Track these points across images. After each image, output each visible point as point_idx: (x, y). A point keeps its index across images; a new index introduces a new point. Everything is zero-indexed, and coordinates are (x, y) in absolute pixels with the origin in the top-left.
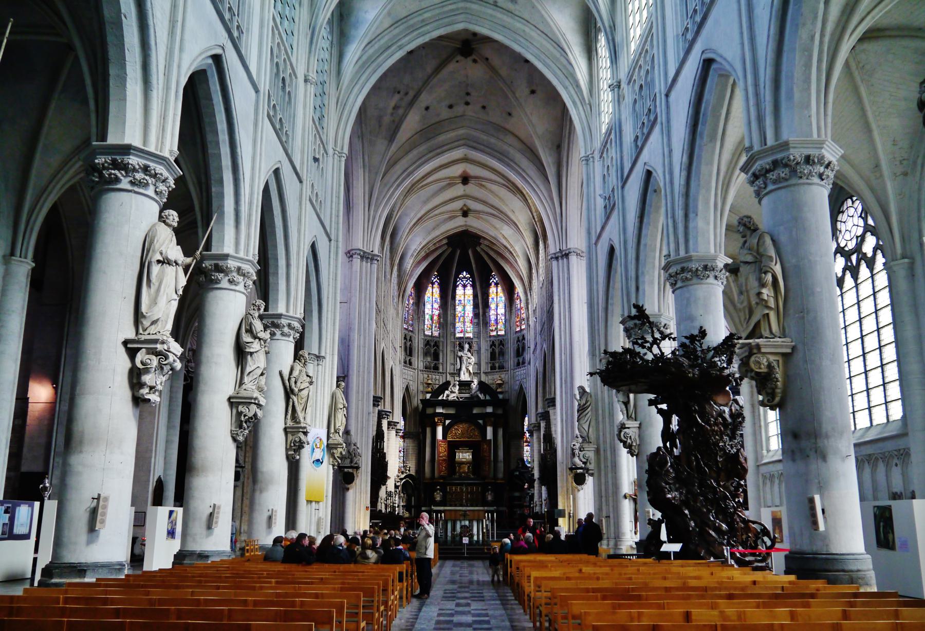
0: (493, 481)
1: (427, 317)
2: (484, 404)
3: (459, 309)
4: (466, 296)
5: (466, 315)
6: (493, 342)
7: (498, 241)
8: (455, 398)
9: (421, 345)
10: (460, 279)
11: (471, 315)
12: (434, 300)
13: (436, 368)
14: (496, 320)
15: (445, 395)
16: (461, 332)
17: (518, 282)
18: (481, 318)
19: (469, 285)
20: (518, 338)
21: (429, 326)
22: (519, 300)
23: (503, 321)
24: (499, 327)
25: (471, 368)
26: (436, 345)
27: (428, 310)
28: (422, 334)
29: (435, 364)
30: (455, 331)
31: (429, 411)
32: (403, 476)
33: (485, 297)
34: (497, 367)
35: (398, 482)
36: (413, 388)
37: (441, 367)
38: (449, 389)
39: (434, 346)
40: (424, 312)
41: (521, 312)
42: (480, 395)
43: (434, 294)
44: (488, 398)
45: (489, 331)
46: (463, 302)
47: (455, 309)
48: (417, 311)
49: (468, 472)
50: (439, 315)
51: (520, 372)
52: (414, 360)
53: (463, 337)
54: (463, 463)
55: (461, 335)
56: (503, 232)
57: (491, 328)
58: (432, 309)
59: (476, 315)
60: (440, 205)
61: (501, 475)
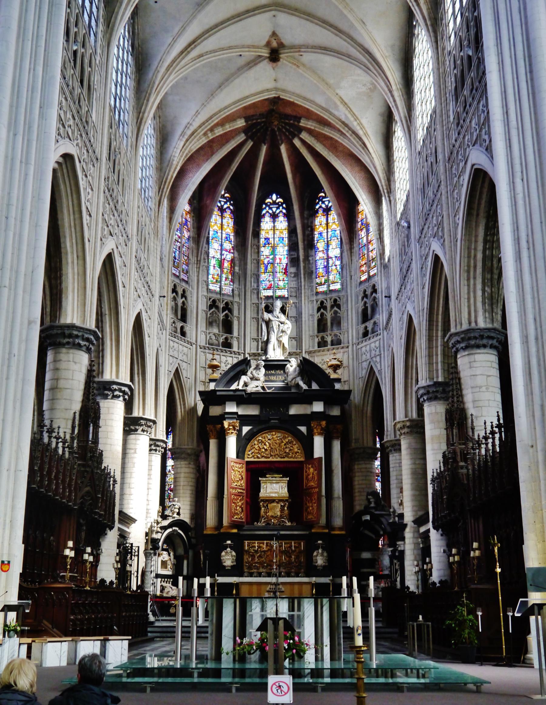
0: (327, 531)
1: (213, 262)
3: (265, 251)
4: (277, 232)
5: (278, 261)
6: (322, 303)
7: (331, 113)
9: (203, 306)
10: (266, 204)
11: (285, 261)
12: (224, 236)
13: (227, 345)
14: (327, 267)
15: (242, 383)
16: (269, 288)
17: (364, 197)
19: (281, 214)
20: (365, 291)
21: (216, 277)
22: (364, 230)
23: (338, 267)
24: (331, 277)
25: (285, 340)
26: (228, 307)
27: (214, 250)
28: (205, 289)
29: (226, 339)
30: (258, 286)
31: (215, 411)
32: (166, 523)
33: (307, 232)
34: (329, 342)
36: (187, 374)
37: (235, 344)
38: (249, 373)
39: (224, 309)
40: (208, 254)
41: (368, 249)
42: (301, 383)
43: (225, 227)
44: (315, 386)
45: (315, 285)
46: (271, 240)
47: (258, 252)
48: (195, 251)
49: (281, 517)
50: (232, 261)
51: (372, 343)
52: (190, 328)
53: (271, 297)
54: (272, 501)
55: (269, 293)
56: (342, 93)
57: (318, 281)
58: (222, 250)
59: (294, 261)
60: (228, 20)
61: (338, 521)
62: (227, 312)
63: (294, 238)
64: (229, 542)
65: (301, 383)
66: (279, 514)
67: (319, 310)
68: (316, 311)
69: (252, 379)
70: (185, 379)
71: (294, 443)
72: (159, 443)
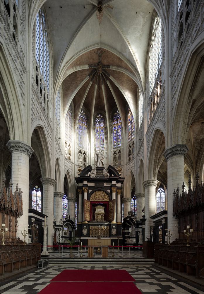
2: (110, 180)
6: (115, 152)
8: (95, 177)
18: (109, 139)
26: (84, 153)
31: (80, 185)
35: (62, 223)
36: (72, 173)
38: (91, 172)
39: (84, 154)
51: (132, 163)
57: (114, 144)
62: (84, 155)
63: (106, 130)
64: (85, 226)
65: (109, 175)
66: (101, 218)
67: (114, 154)
68: (113, 154)
69: (92, 173)
70: (71, 175)
71: (106, 195)
72: (61, 194)
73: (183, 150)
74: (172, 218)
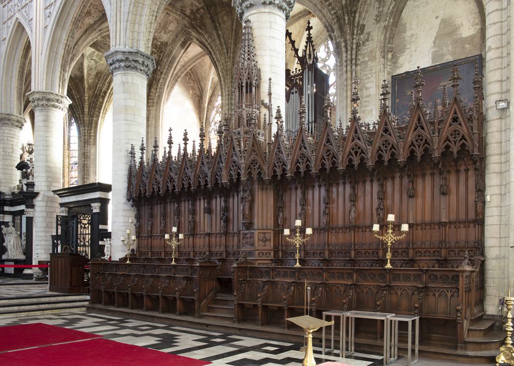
73: (147, 66)
74: (124, 203)
